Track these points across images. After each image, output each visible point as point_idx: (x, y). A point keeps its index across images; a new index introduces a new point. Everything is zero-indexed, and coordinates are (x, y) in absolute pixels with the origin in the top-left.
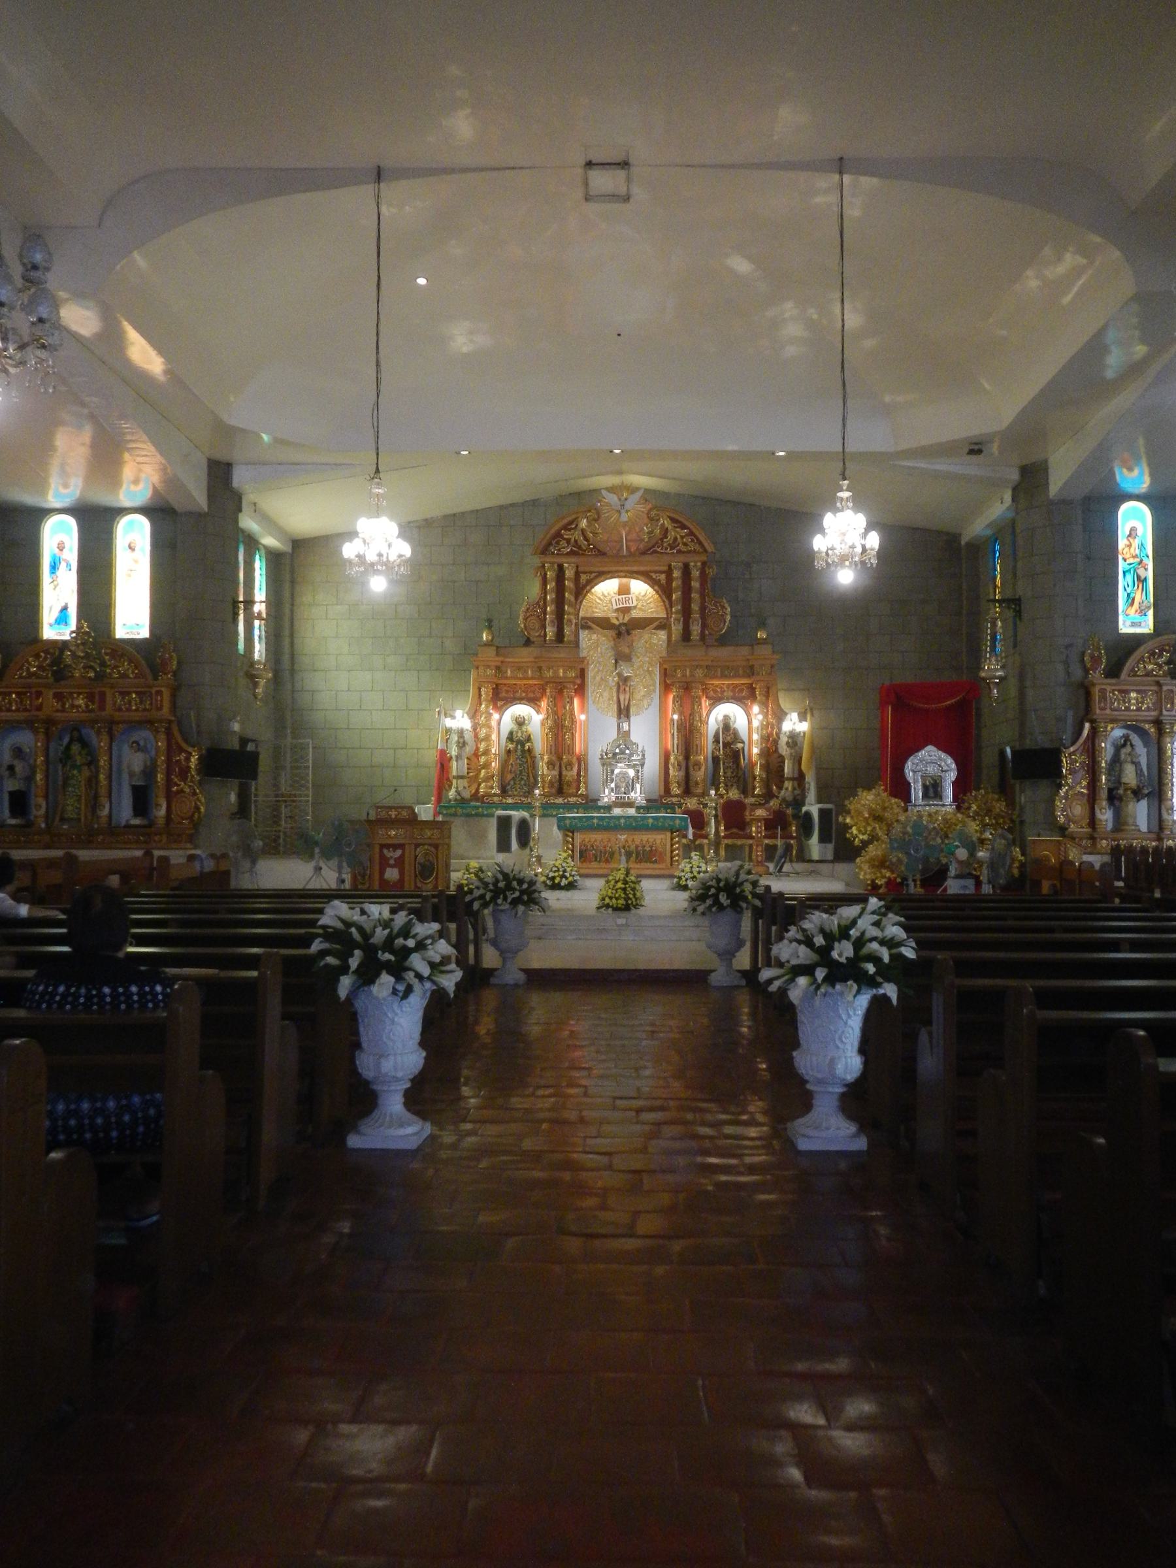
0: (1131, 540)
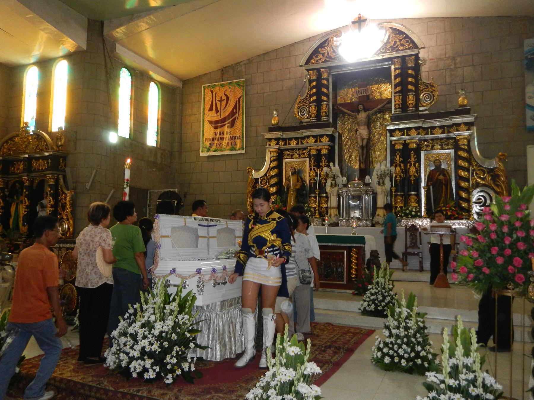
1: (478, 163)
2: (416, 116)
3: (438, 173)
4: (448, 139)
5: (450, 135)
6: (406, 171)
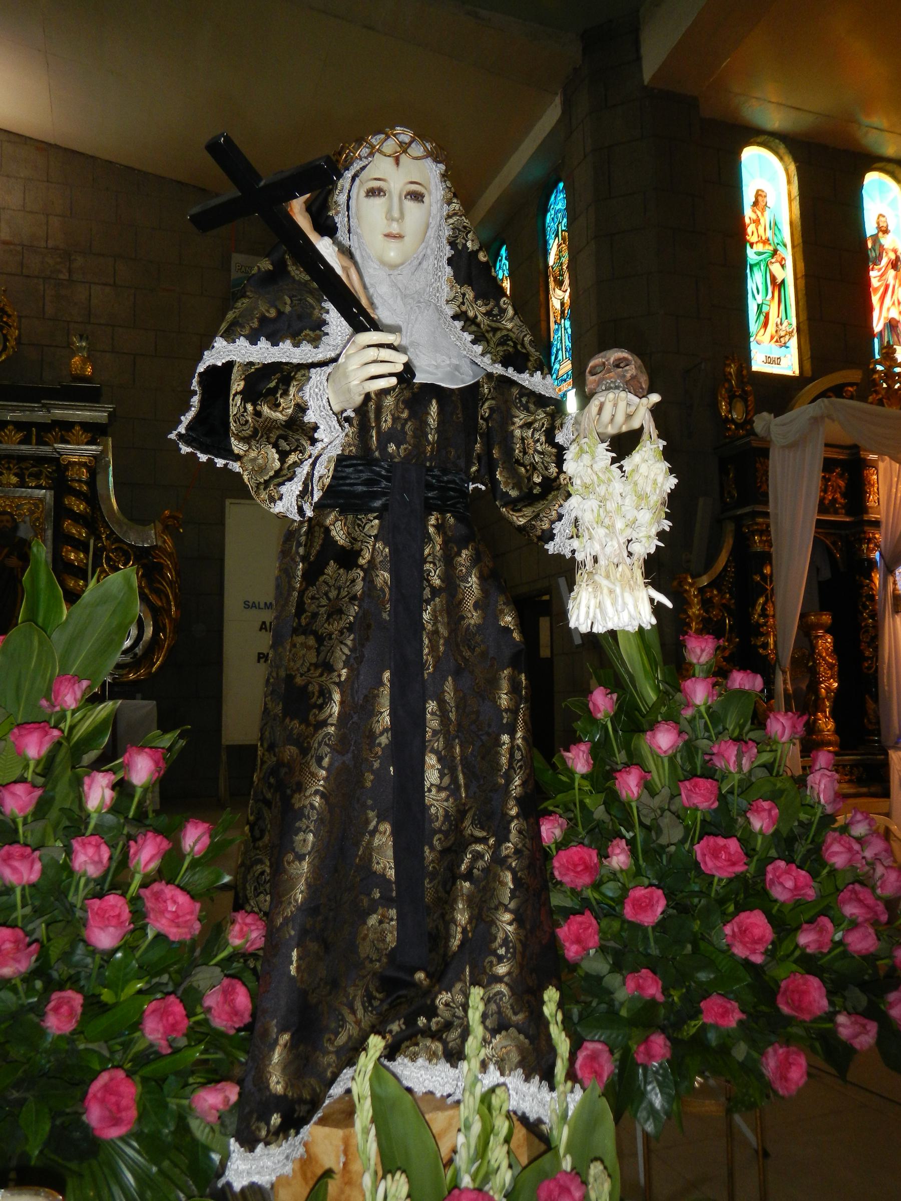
0: (759, 213)
1: (112, 532)
3: (6, 551)
4: (41, 460)
5: (45, 450)
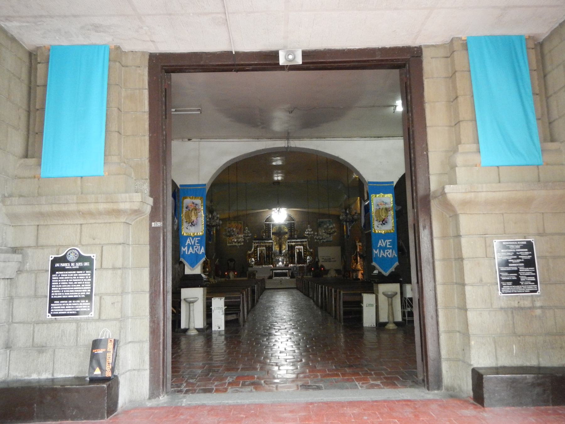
2: (294, 239)
6: (292, 252)
